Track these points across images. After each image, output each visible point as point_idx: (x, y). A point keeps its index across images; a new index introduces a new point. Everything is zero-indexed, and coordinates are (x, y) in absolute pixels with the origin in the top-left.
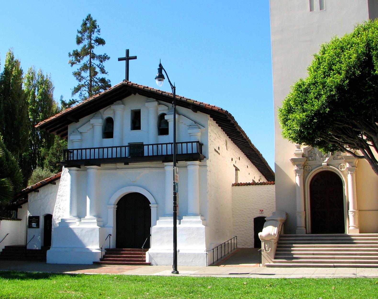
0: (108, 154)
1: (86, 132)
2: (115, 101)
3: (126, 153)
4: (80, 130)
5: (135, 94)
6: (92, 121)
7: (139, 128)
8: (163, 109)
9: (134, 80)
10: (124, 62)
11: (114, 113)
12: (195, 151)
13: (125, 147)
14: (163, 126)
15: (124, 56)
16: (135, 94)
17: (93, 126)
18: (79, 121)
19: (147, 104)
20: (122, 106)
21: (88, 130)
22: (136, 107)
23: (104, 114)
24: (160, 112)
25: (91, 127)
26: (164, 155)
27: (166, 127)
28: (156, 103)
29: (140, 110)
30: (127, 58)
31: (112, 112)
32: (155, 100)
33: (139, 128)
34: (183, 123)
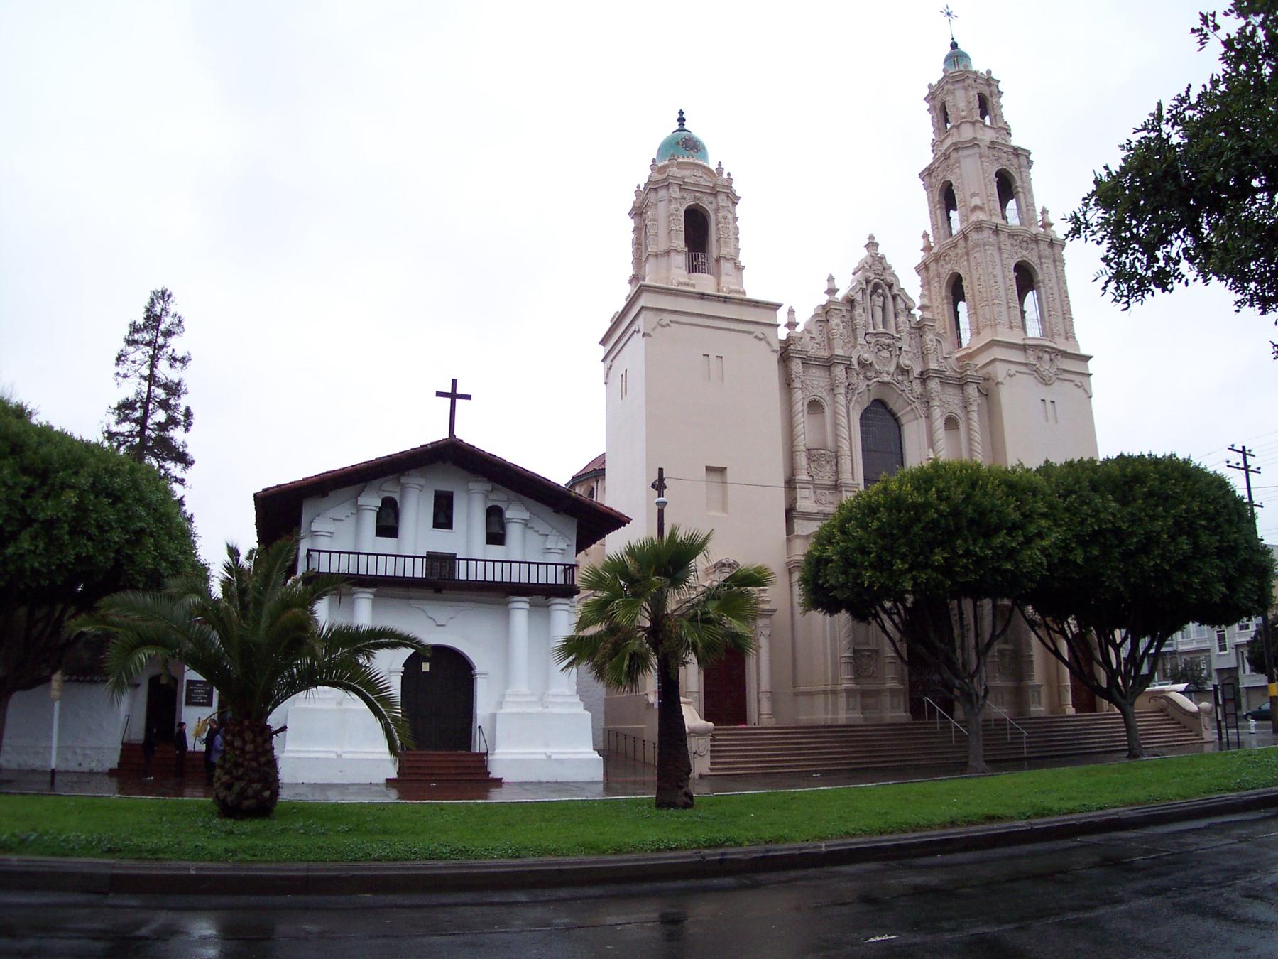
0: (385, 568)
1: (342, 520)
2: (409, 468)
3: (418, 570)
4: (332, 513)
5: (444, 463)
6: (361, 501)
7: (449, 525)
8: (498, 499)
9: (468, 434)
10: (448, 400)
11: (403, 489)
12: (560, 581)
13: (423, 557)
14: (496, 529)
15: (449, 390)
16: (444, 463)
17: (359, 509)
18: (328, 495)
19: (471, 486)
20: (422, 481)
21: (347, 516)
22: (444, 487)
23: (383, 489)
24: (490, 504)
25: (355, 512)
26: (497, 582)
27: (501, 532)
28: (489, 487)
29: (452, 493)
30: (453, 396)
31: (398, 489)
32: (486, 479)
33: (449, 525)
34: (533, 528)
